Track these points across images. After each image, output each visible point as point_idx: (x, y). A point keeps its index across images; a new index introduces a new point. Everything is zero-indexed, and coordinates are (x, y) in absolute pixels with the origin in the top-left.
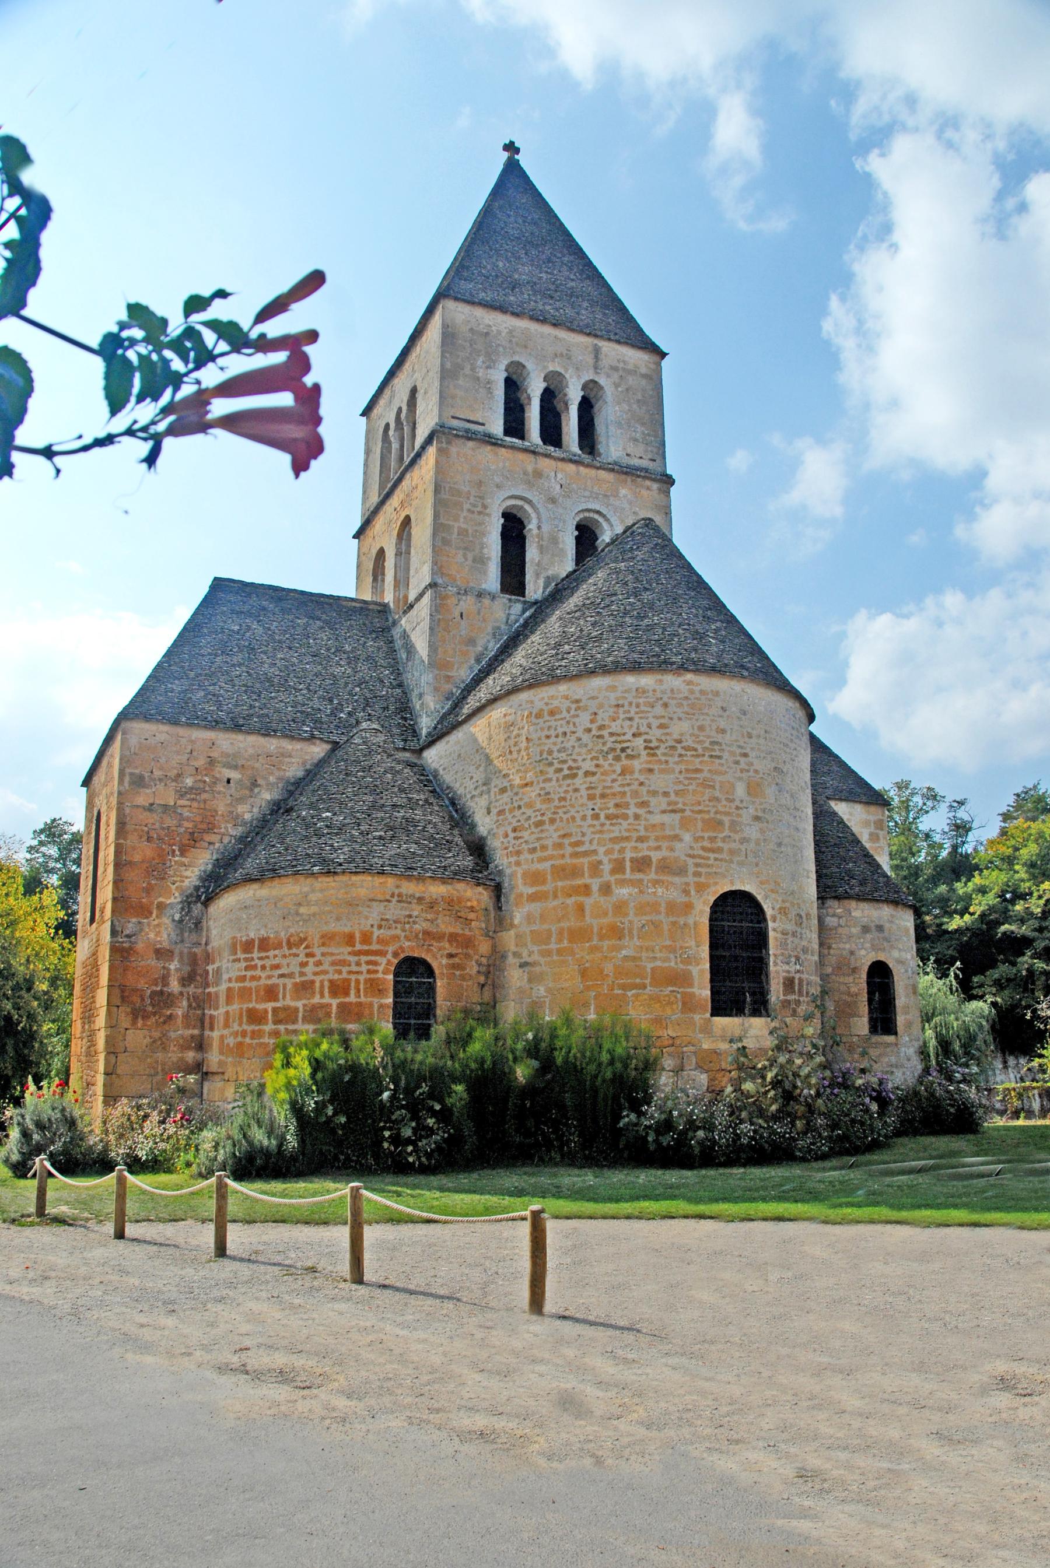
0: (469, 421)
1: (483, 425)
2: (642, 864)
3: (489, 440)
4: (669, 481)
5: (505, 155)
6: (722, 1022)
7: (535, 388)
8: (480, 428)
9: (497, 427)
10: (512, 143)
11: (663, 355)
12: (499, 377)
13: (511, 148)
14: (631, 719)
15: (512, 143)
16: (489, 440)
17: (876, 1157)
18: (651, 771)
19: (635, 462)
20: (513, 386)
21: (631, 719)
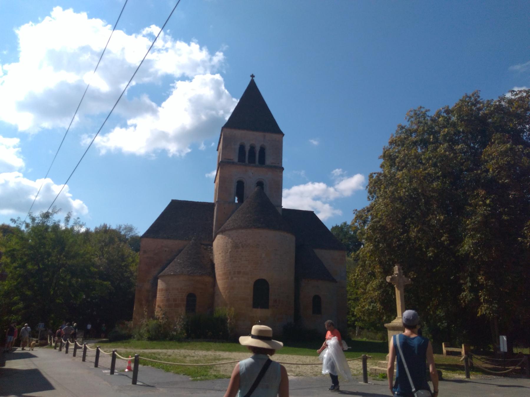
0: (229, 159)
1: (232, 160)
2: (239, 273)
3: (233, 163)
4: (283, 169)
5: (251, 78)
6: (255, 310)
7: (247, 149)
8: (232, 161)
9: (236, 160)
10: (253, 75)
11: (283, 135)
12: (237, 147)
13: (253, 76)
14: (239, 239)
15: (253, 75)
16: (233, 163)
17: (395, 363)
18: (242, 251)
19: (274, 165)
20: (242, 148)
21: (239, 239)
